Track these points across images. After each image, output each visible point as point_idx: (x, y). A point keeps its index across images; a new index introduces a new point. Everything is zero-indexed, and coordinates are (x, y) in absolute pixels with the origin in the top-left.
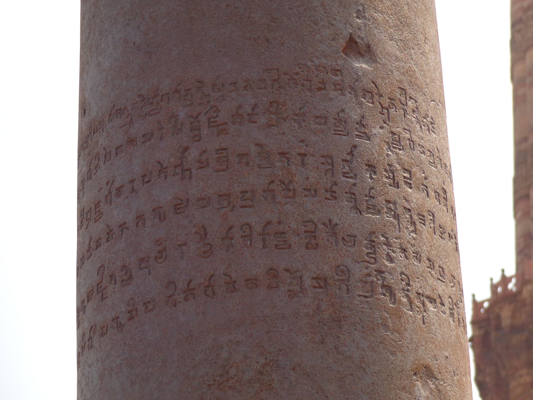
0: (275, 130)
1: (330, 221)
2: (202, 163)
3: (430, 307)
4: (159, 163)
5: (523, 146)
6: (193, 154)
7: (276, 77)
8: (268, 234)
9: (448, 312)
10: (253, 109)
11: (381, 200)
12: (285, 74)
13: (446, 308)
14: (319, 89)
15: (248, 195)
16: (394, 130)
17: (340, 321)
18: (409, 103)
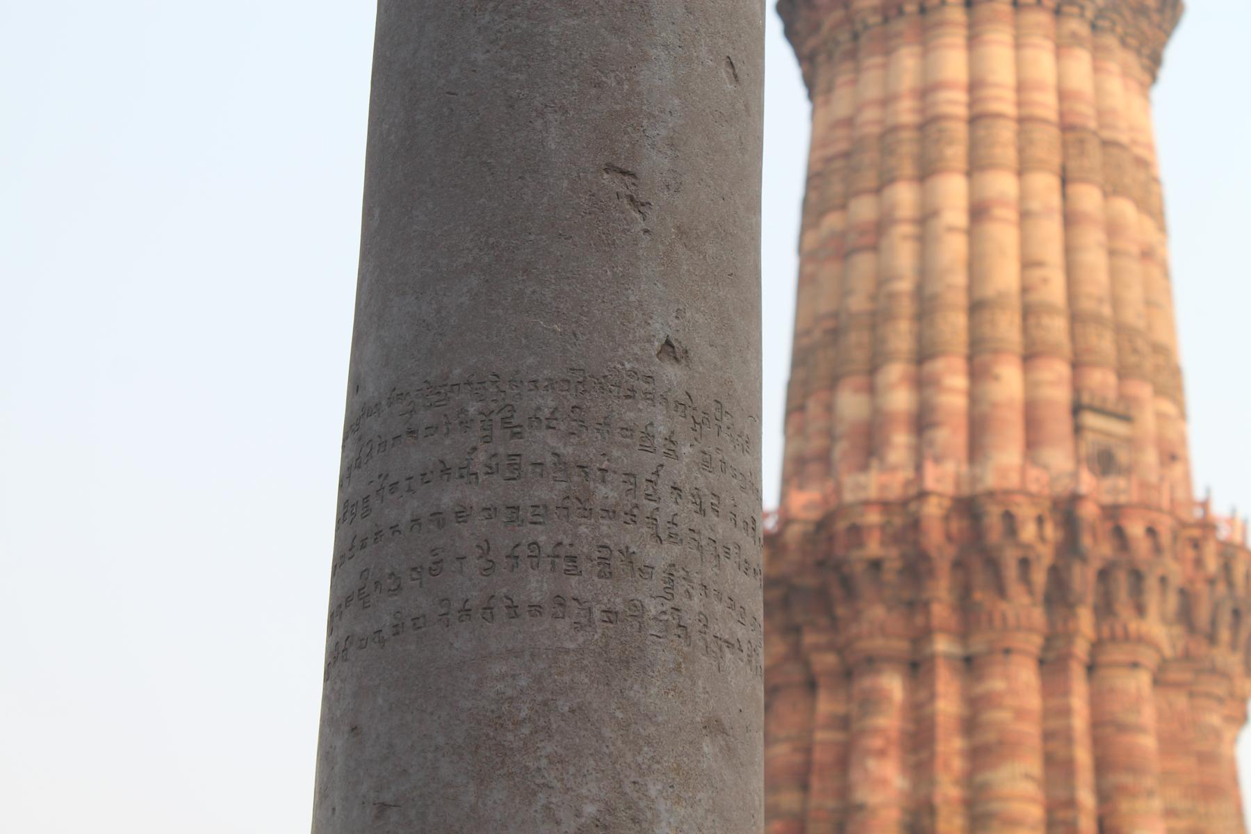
0: (574, 440)
1: (627, 548)
2: (491, 468)
3: (728, 655)
4: (442, 462)
5: (806, 341)
6: (481, 457)
7: (581, 379)
8: (558, 556)
9: (745, 659)
10: (552, 413)
11: (683, 529)
12: (592, 376)
13: (744, 655)
14: (627, 397)
15: (541, 511)
16: (706, 449)
17: (628, 662)
18: (725, 419)
